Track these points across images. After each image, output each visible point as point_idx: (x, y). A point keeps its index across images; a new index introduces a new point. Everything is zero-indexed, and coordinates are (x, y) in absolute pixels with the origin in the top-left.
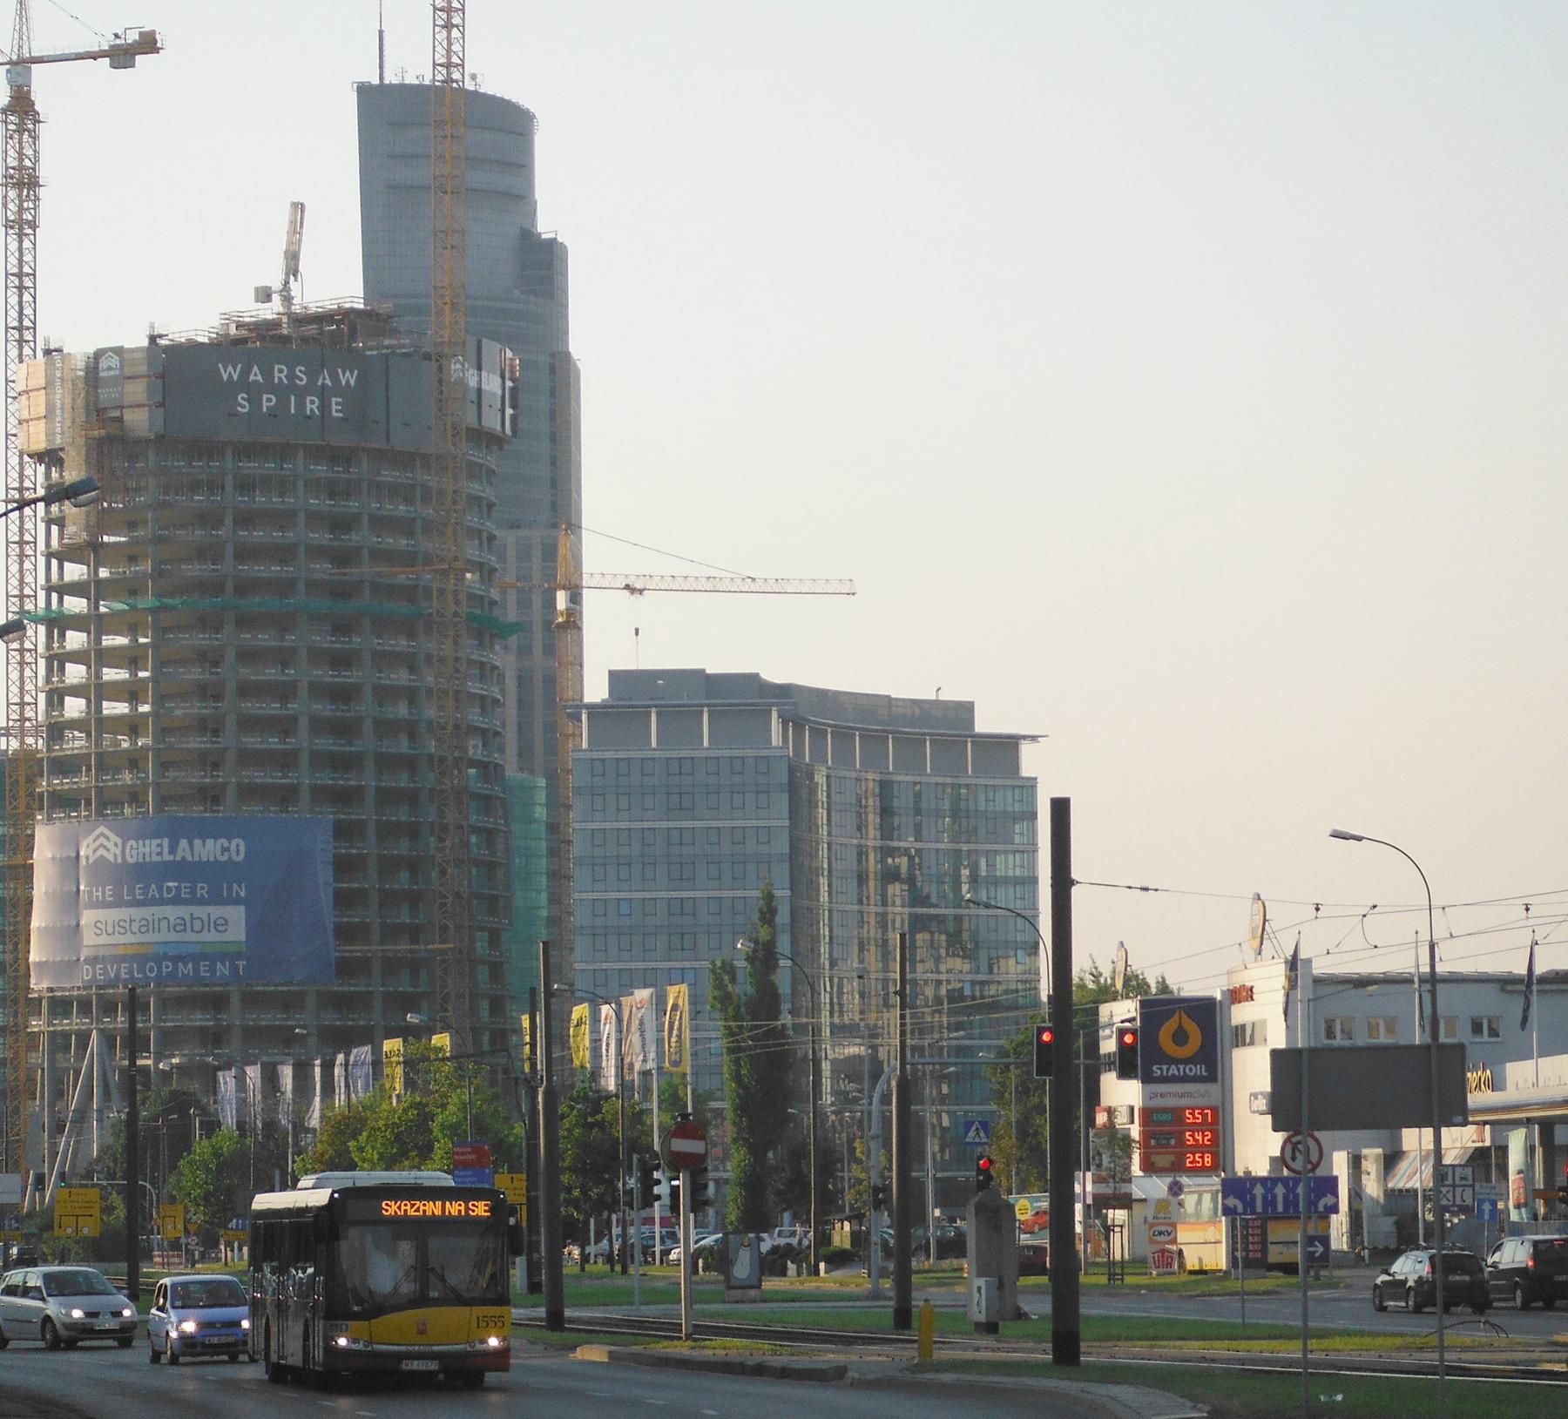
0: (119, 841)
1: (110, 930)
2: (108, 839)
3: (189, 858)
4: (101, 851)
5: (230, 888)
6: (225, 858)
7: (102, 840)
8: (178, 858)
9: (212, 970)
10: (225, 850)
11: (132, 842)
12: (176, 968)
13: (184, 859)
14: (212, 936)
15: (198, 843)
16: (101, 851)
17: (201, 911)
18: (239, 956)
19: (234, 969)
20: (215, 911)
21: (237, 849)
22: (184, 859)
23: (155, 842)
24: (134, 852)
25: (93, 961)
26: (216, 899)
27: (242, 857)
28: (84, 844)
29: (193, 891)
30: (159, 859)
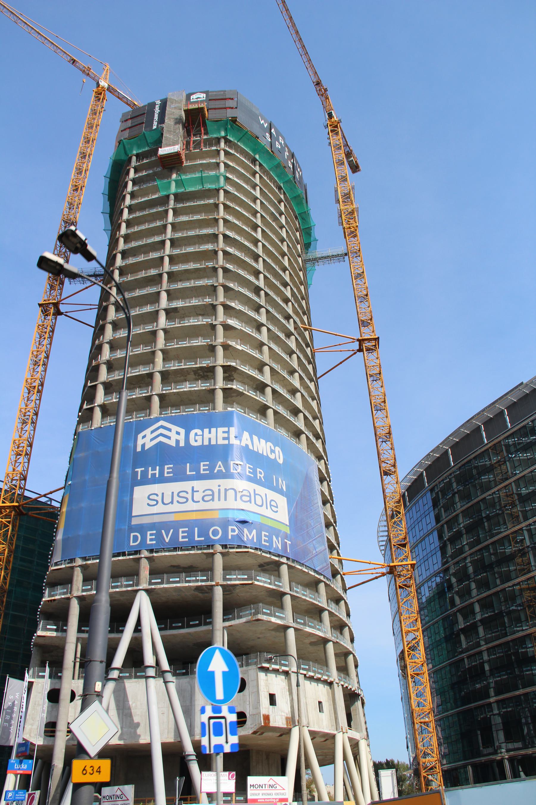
0: (182, 431)
1: (167, 500)
2: (170, 430)
3: (251, 447)
4: (161, 439)
5: (277, 481)
6: (272, 456)
7: (161, 431)
8: (243, 444)
9: (270, 541)
10: (272, 451)
11: (199, 432)
12: (241, 532)
13: (247, 445)
14: (269, 513)
15: (255, 438)
16: (161, 439)
17: (262, 490)
18: (286, 536)
19: (284, 545)
20: (272, 495)
21: (279, 456)
22: (247, 445)
23: (220, 430)
24: (199, 438)
25: (142, 529)
26: (268, 484)
27: (281, 461)
28: (140, 436)
29: (254, 472)
30: (226, 442)
